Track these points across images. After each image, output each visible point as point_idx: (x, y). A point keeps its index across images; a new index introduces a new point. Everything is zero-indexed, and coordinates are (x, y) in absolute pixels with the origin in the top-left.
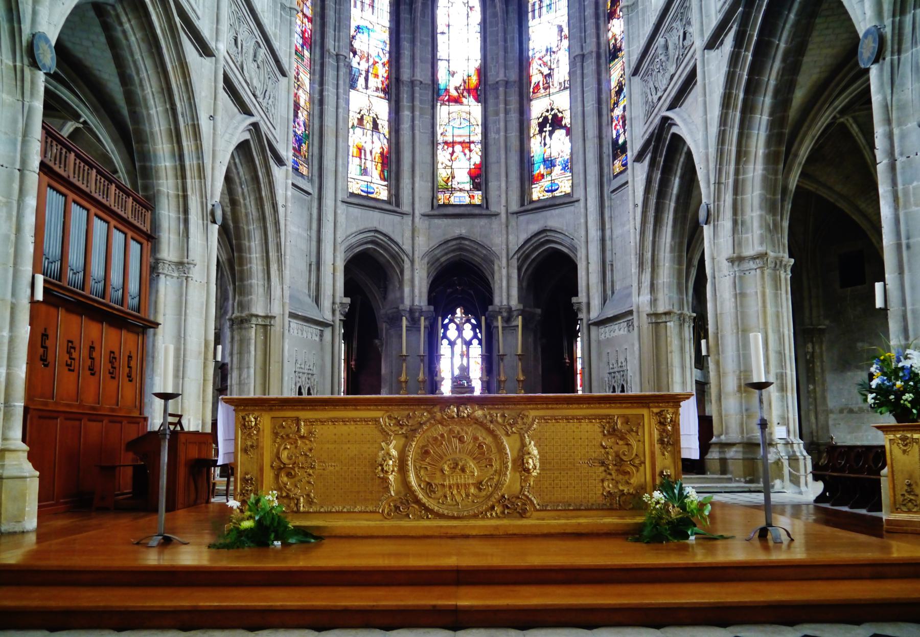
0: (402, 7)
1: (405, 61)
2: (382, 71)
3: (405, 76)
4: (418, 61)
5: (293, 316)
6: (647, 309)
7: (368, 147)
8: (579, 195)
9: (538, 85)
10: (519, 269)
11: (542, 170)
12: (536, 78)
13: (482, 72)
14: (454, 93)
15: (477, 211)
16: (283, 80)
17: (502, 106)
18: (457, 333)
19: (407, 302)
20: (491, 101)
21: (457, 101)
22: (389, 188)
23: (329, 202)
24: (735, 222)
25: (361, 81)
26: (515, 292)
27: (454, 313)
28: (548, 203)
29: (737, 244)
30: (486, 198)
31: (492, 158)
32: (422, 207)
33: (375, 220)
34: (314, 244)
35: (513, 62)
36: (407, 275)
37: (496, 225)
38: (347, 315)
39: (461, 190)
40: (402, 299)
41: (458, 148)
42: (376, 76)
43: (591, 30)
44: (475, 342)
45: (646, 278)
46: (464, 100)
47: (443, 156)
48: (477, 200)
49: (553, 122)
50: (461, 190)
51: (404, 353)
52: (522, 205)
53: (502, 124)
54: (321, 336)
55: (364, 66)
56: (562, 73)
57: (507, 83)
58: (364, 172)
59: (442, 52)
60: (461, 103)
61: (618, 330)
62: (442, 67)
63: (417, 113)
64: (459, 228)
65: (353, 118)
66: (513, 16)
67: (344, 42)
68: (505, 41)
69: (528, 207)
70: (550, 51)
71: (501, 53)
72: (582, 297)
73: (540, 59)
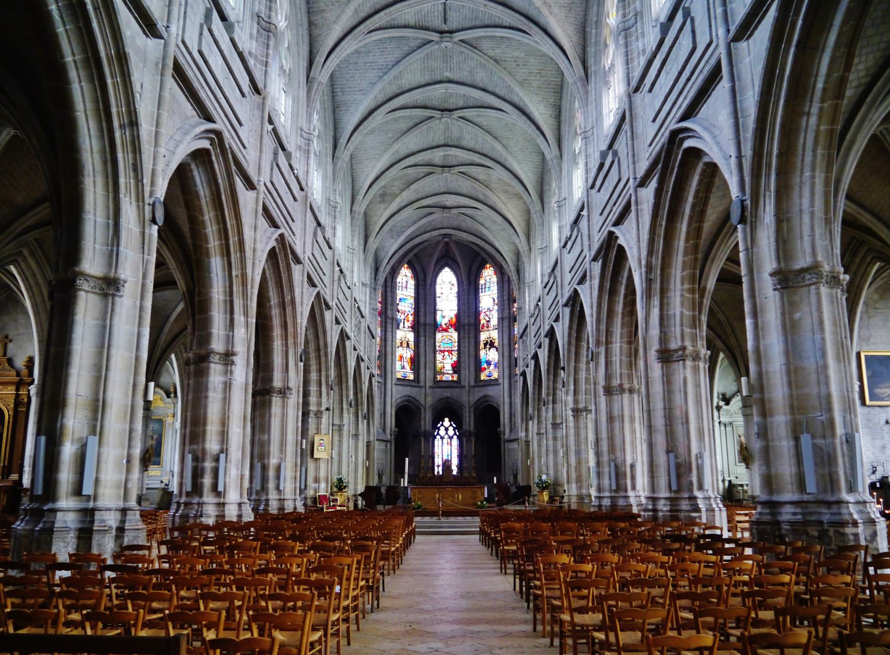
0: (420, 287)
1: (422, 313)
2: (411, 318)
3: (422, 320)
4: (427, 314)
5: (377, 440)
6: (524, 439)
8: (501, 381)
9: (483, 325)
10: (474, 413)
11: (485, 365)
12: (483, 322)
13: (458, 316)
14: (444, 326)
15: (455, 385)
16: (374, 340)
17: (467, 335)
18: (445, 432)
19: (423, 428)
20: (462, 332)
21: (446, 330)
23: (389, 386)
24: (538, 421)
25: (402, 324)
26: (472, 423)
27: (443, 421)
28: (487, 383)
29: (539, 429)
30: (459, 378)
31: (462, 360)
32: (429, 383)
33: (408, 391)
34: (383, 405)
35: (472, 314)
36: (423, 416)
37: (465, 392)
38: (395, 436)
39: (448, 374)
40: (420, 426)
41: (446, 353)
42: (408, 321)
43: (506, 307)
44: (455, 437)
45: (524, 426)
46: (450, 330)
47: (439, 357)
48: (455, 379)
49: (490, 344)
50: (448, 374)
51: (423, 454)
52: (476, 382)
53: (467, 344)
54: (386, 446)
55: (403, 317)
56: (494, 321)
57: (469, 325)
58: (403, 367)
59: (439, 306)
60: (448, 332)
61: (514, 445)
63: (427, 339)
64: (447, 393)
66: (472, 291)
67: (395, 308)
68: (468, 303)
69: (480, 384)
70: (489, 310)
71: (467, 310)
72: (502, 428)
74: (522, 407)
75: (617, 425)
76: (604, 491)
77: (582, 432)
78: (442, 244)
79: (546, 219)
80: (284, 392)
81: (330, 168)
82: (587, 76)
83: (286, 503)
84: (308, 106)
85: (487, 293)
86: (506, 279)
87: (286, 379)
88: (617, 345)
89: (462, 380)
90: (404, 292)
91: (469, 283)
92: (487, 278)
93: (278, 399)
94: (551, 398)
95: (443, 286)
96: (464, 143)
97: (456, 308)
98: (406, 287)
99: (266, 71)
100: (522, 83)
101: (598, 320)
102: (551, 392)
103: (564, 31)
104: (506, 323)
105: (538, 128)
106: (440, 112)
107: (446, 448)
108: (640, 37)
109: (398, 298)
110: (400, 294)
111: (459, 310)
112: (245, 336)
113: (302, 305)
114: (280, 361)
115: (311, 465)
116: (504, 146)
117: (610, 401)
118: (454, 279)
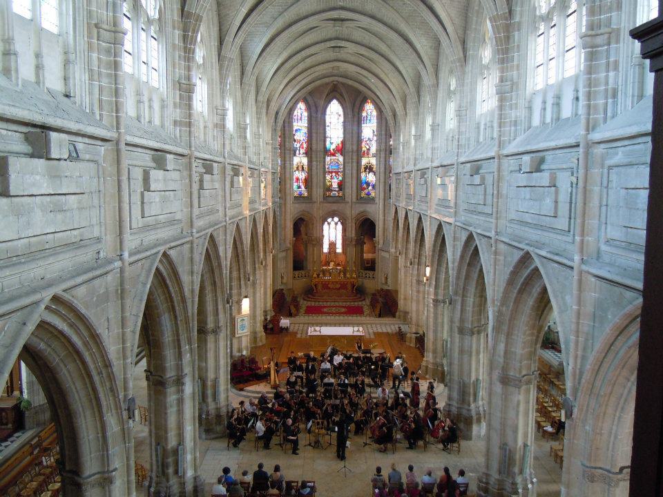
1: (314, 142)
2: (305, 146)
3: (314, 147)
7: (300, 178)
8: (377, 200)
12: (364, 149)
13: (343, 143)
14: (332, 151)
20: (346, 158)
22: (308, 192)
25: (298, 152)
26: (354, 232)
33: (303, 207)
41: (334, 174)
42: (303, 148)
43: (384, 140)
44: (339, 223)
47: (328, 177)
48: (341, 195)
49: (369, 169)
55: (298, 145)
56: (373, 150)
58: (299, 187)
59: (328, 134)
62: (328, 140)
65: (295, 166)
66: (356, 123)
70: (369, 139)
73: (366, 141)
74: (393, 230)
75: (466, 357)
76: (453, 400)
77: (440, 317)
78: (332, 84)
79: (421, 111)
80: (216, 331)
81: (239, 94)
82: (465, 57)
83: (221, 410)
84: (221, 83)
85: (368, 125)
86: (384, 121)
87: (217, 321)
88: (470, 300)
89: (346, 195)
90: (300, 124)
91: (354, 116)
92: (369, 111)
93: (212, 336)
94: (417, 260)
95: (332, 116)
96: (353, 38)
97: (342, 136)
98: (301, 119)
99: (190, 132)
100: (406, 20)
101: (458, 278)
102: (417, 256)
103: (449, 15)
104: (383, 155)
105: (420, 57)
106: (333, 22)
107: (332, 230)
108: (514, 107)
109: (295, 128)
110: (296, 125)
111: (344, 137)
112: (190, 359)
113: (226, 260)
114: (211, 308)
115: (235, 342)
116: (387, 45)
117: (462, 339)
118: (341, 111)
